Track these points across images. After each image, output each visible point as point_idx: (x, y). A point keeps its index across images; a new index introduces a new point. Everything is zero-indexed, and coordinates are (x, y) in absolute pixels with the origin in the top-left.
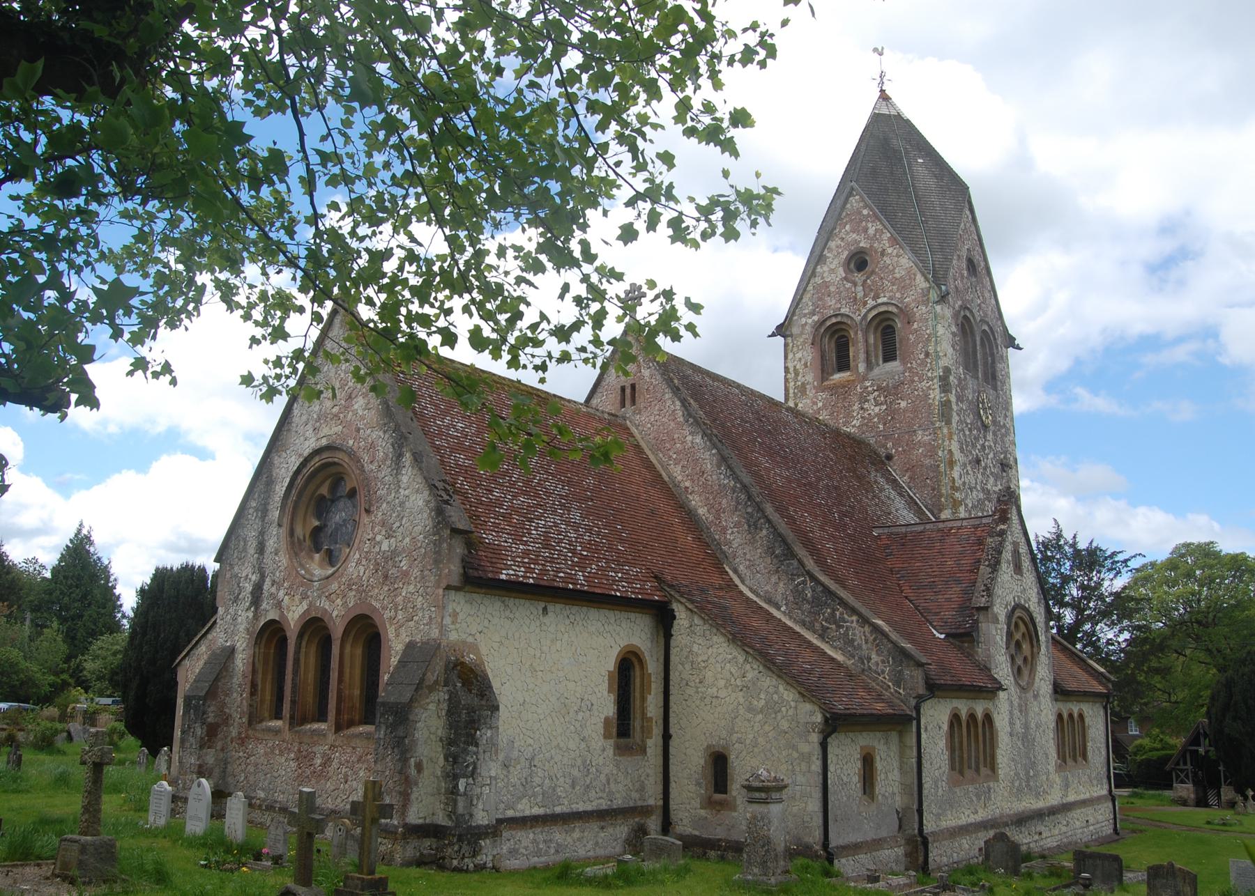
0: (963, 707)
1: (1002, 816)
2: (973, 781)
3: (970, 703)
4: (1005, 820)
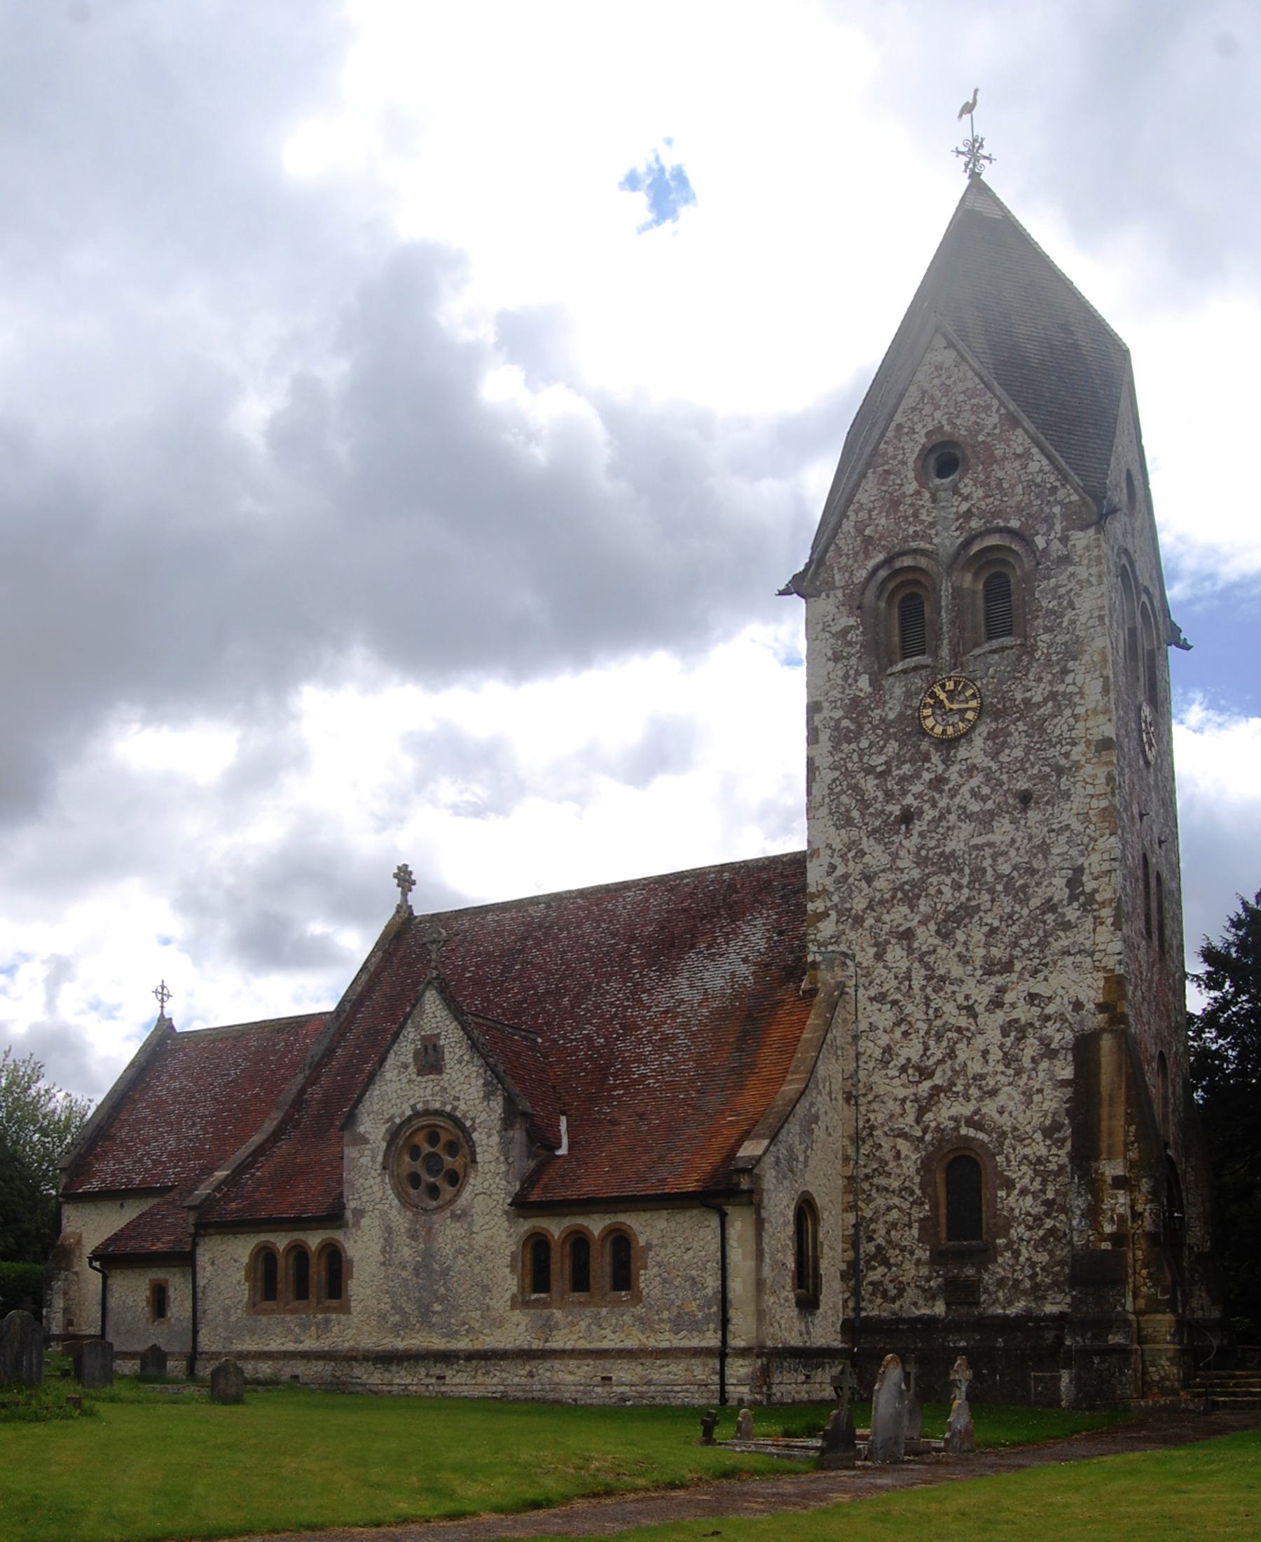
0: (281, 1241)
1: (352, 1349)
2: (293, 1311)
3: (297, 1235)
4: (354, 1354)
